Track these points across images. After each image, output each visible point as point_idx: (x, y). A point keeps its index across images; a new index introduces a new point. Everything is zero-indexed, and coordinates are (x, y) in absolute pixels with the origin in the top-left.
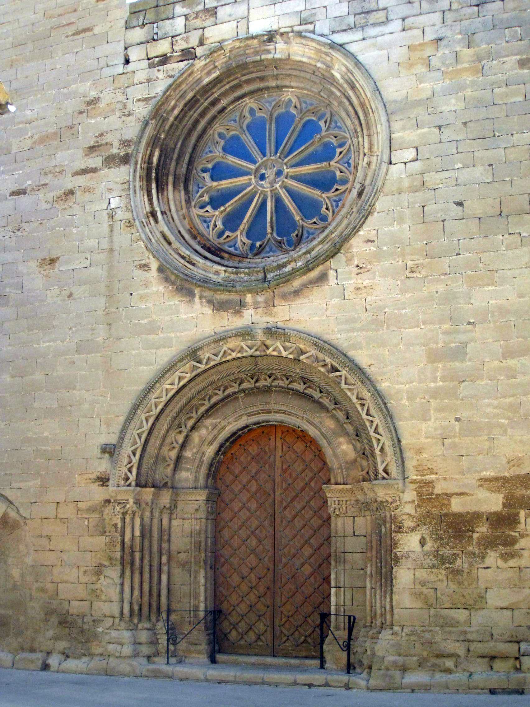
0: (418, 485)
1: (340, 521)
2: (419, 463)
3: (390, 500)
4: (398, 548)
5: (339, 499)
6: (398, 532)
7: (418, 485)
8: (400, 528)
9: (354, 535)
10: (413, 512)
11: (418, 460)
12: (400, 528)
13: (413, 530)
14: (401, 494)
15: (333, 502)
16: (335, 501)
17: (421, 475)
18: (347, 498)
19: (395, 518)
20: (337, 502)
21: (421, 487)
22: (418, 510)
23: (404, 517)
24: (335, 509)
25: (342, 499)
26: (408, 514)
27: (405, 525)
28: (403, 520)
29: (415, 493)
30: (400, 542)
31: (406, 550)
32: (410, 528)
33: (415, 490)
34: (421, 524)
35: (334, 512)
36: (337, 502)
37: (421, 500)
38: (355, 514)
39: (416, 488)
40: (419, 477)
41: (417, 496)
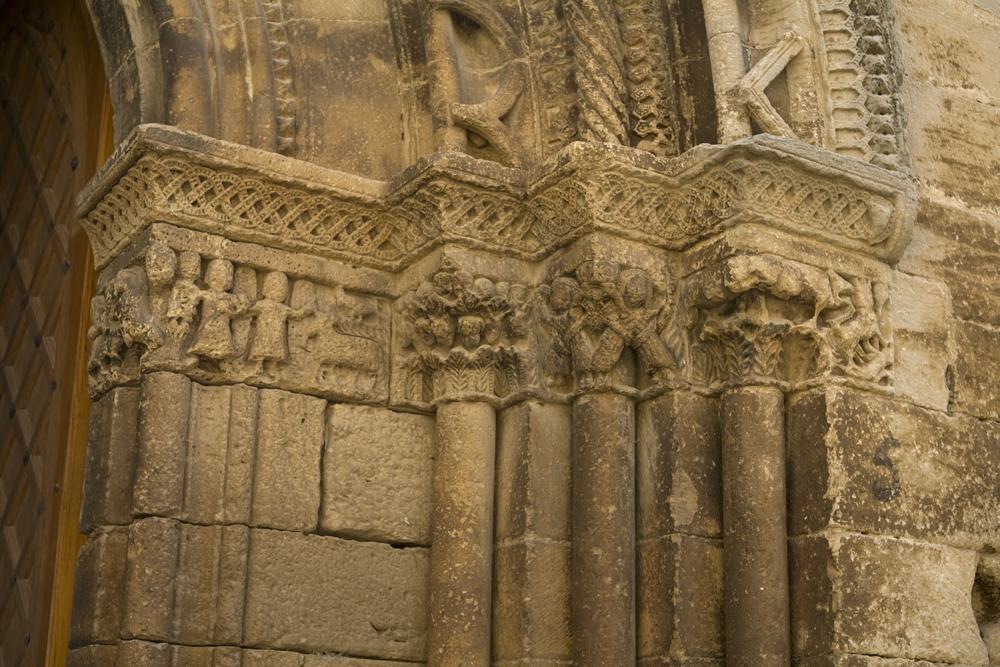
0: (954, 247)
1: (215, 410)
2: (954, 120)
3: (825, 296)
4: (872, 629)
5: (248, 253)
6: (866, 520)
7: (954, 247)
8: (881, 492)
9: (320, 531)
10: (936, 397)
11: (948, 104)
12: (881, 492)
13: (945, 516)
14: (885, 274)
15: (191, 266)
16: (205, 261)
17: (971, 197)
18: (302, 264)
19: (854, 423)
20: (220, 271)
21: (970, 263)
22: (965, 395)
23: (900, 424)
24: (197, 319)
25: (263, 257)
26: (916, 411)
27: (905, 477)
28: (896, 444)
29: (942, 287)
30: (884, 589)
31: (915, 651)
32: (927, 501)
33: (945, 268)
34: (983, 492)
35: (190, 339)
36: (220, 271)
37: (974, 338)
38: (333, 383)
39: (947, 262)
40: (957, 203)
41: (958, 311)
